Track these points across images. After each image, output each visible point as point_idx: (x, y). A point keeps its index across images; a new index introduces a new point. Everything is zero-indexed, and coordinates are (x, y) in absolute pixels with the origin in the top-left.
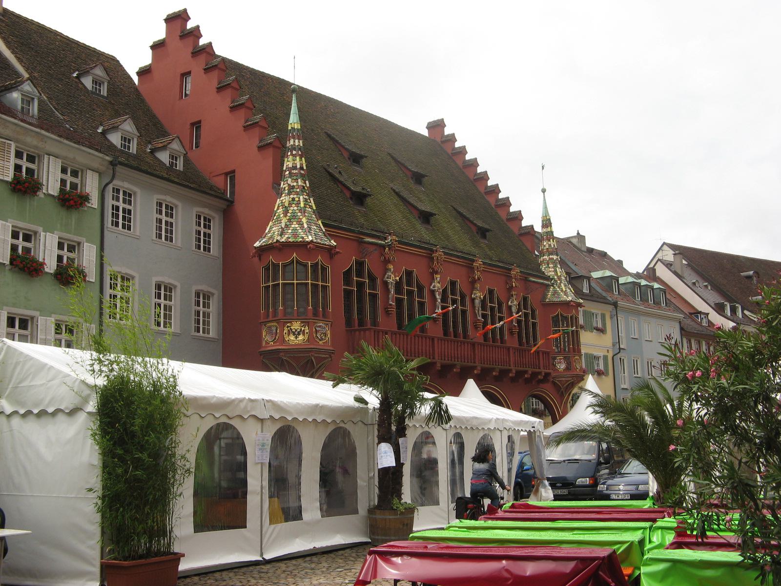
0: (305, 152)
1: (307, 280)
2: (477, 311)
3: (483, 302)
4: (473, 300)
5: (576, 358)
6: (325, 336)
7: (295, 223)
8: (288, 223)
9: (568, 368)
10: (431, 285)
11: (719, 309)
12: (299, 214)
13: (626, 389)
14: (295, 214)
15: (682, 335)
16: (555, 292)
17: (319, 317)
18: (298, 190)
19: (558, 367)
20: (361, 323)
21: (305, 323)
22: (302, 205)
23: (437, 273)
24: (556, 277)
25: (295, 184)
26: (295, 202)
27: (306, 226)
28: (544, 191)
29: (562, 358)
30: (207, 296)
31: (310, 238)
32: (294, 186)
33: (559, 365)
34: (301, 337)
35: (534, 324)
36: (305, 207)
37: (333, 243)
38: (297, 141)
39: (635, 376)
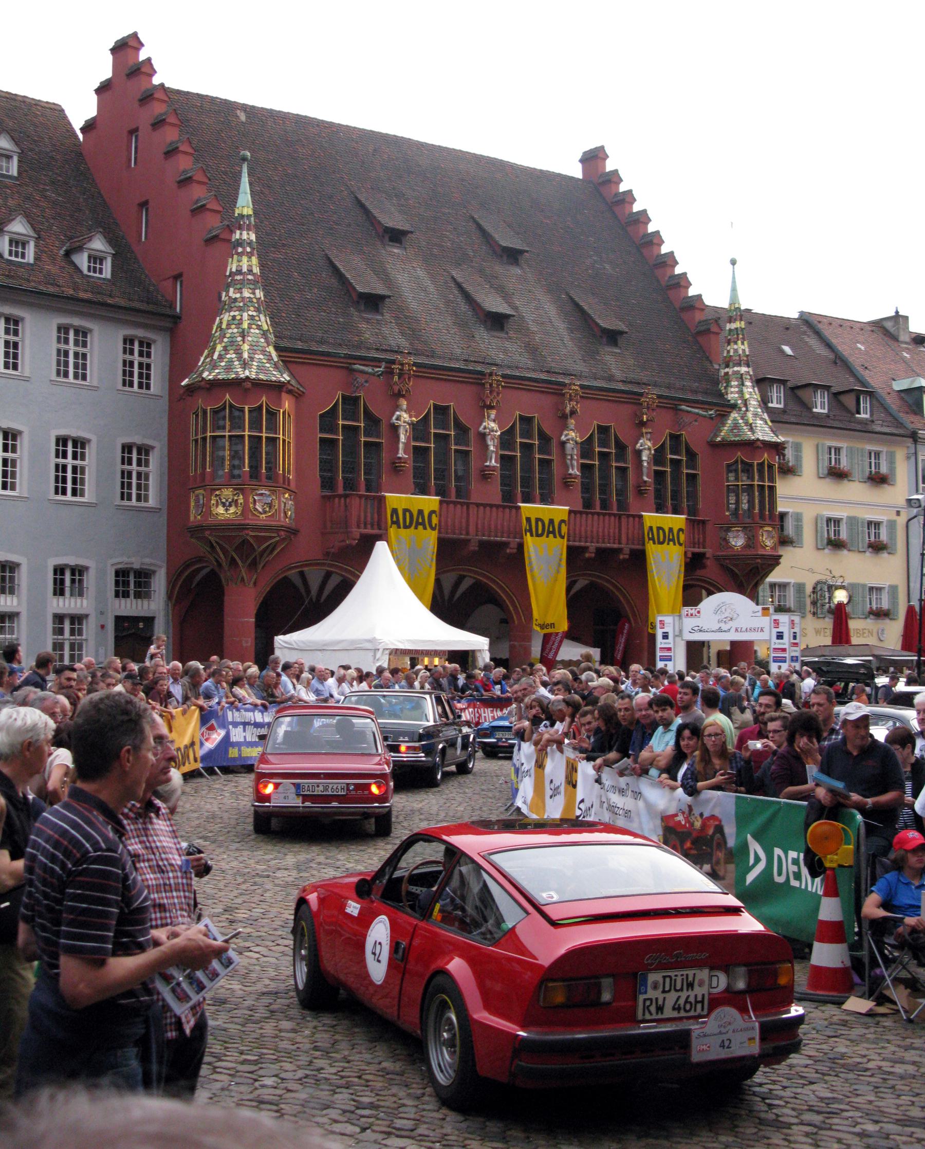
0: (263, 249)
1: (266, 429)
2: (568, 462)
6: (270, 508)
7: (232, 352)
8: (223, 353)
9: (747, 546)
12: (239, 339)
14: (234, 340)
16: (736, 426)
17: (260, 481)
18: (241, 304)
20: (350, 484)
21: (240, 489)
22: (245, 325)
23: (491, 407)
24: (739, 402)
25: (238, 295)
26: (236, 322)
27: (246, 355)
28: (733, 262)
30: (144, 450)
31: (247, 373)
32: (236, 299)
34: (232, 510)
35: (692, 478)
36: (250, 328)
37: (286, 377)
38: (245, 233)
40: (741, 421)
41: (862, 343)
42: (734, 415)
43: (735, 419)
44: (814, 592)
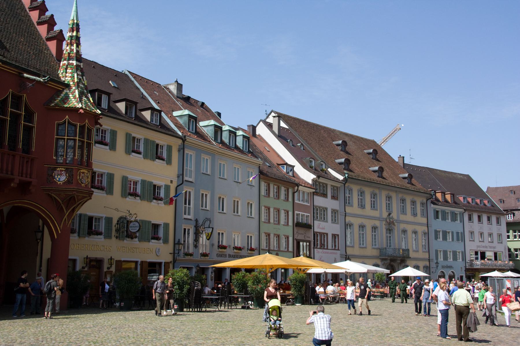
5: (81, 171)
9: (68, 182)
13: (191, 220)
19: (58, 179)
24: (71, 83)
29: (63, 169)
33: (59, 177)
41: (157, 92)
44: (117, 224)
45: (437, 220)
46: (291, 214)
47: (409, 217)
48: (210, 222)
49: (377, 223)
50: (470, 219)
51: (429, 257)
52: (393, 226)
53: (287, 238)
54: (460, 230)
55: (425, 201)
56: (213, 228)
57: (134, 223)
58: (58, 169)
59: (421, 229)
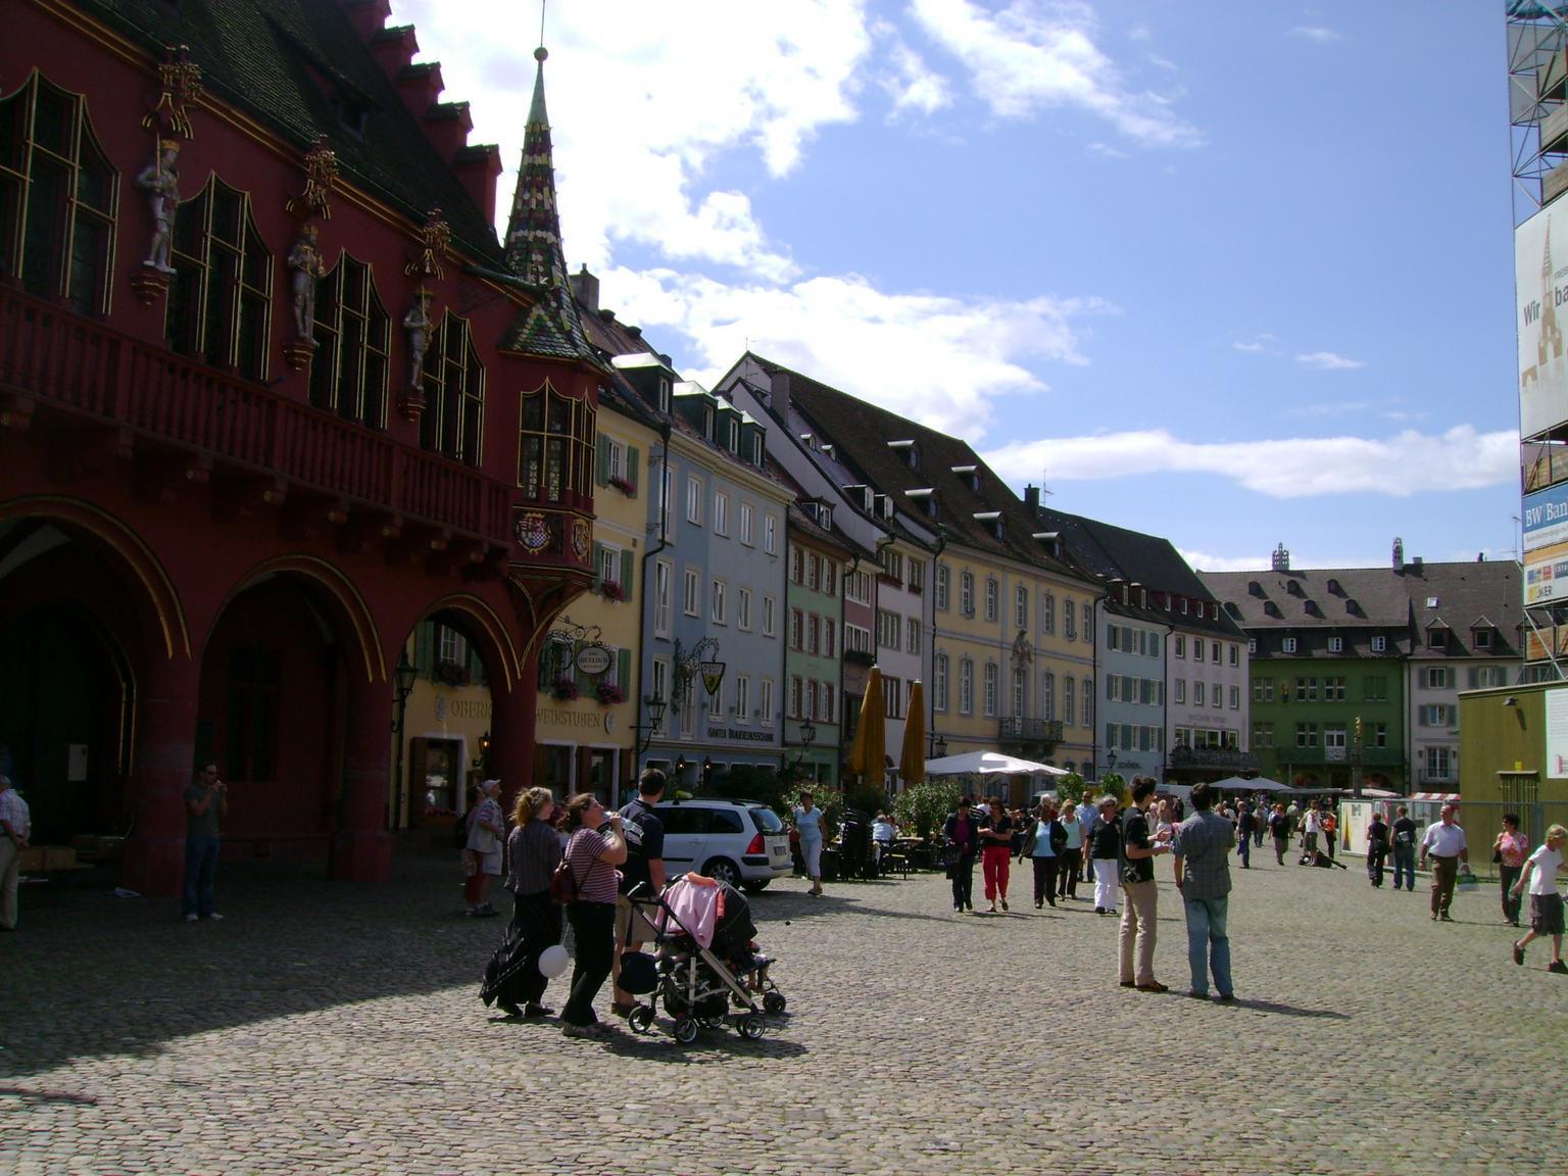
2: (298, 312)
3: (324, 287)
4: (289, 274)
10: (141, 170)
11: (855, 499)
15: (788, 537)
16: (541, 329)
19: (527, 541)
28: (541, 55)
29: (539, 516)
33: (530, 534)
39: (686, 612)
40: (550, 324)
42: (537, 311)
43: (539, 317)
45: (1114, 650)
46: (837, 627)
47: (1057, 643)
48: (717, 649)
49: (995, 655)
50: (1198, 652)
51: (1094, 742)
52: (1028, 663)
53: (830, 688)
54: (1156, 677)
55: (1091, 601)
56: (724, 664)
57: (594, 650)
58: (529, 515)
59: (1082, 672)
